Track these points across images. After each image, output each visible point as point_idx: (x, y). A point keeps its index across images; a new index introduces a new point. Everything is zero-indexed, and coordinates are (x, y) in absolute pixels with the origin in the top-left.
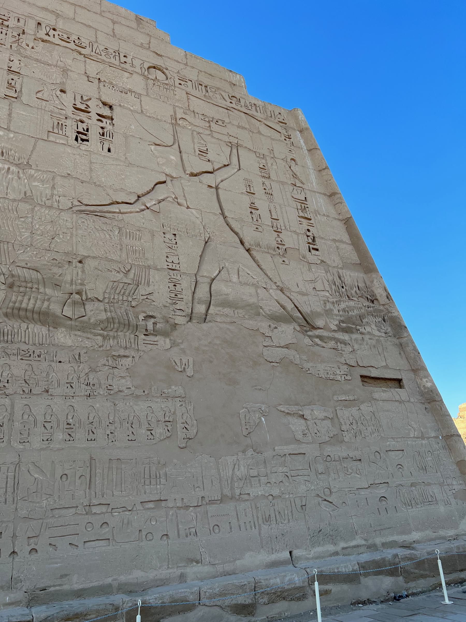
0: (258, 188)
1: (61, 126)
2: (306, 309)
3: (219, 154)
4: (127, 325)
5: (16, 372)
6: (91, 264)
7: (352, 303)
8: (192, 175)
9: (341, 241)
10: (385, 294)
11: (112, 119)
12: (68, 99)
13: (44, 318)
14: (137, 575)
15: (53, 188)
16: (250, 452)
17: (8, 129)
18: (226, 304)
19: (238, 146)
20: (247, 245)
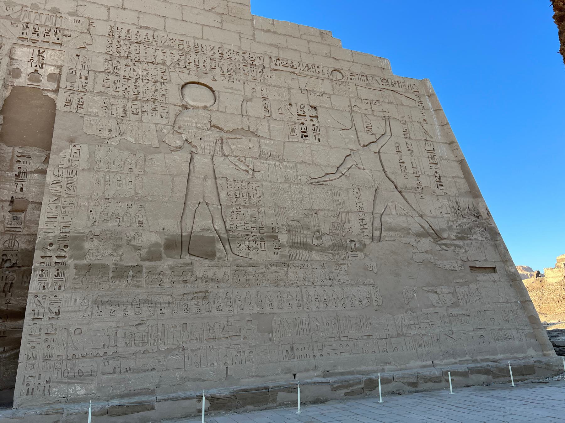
0: (404, 148)
1: (293, 130)
2: (436, 227)
3: (378, 129)
4: (343, 247)
5: (299, 275)
6: (321, 214)
7: (464, 220)
8: (364, 146)
9: (458, 177)
10: (486, 212)
11: (317, 117)
12: (294, 110)
13: (305, 246)
14: (363, 368)
15: (297, 171)
16: (409, 312)
17: (270, 139)
18: (390, 229)
19: (389, 118)
20: (399, 188)
